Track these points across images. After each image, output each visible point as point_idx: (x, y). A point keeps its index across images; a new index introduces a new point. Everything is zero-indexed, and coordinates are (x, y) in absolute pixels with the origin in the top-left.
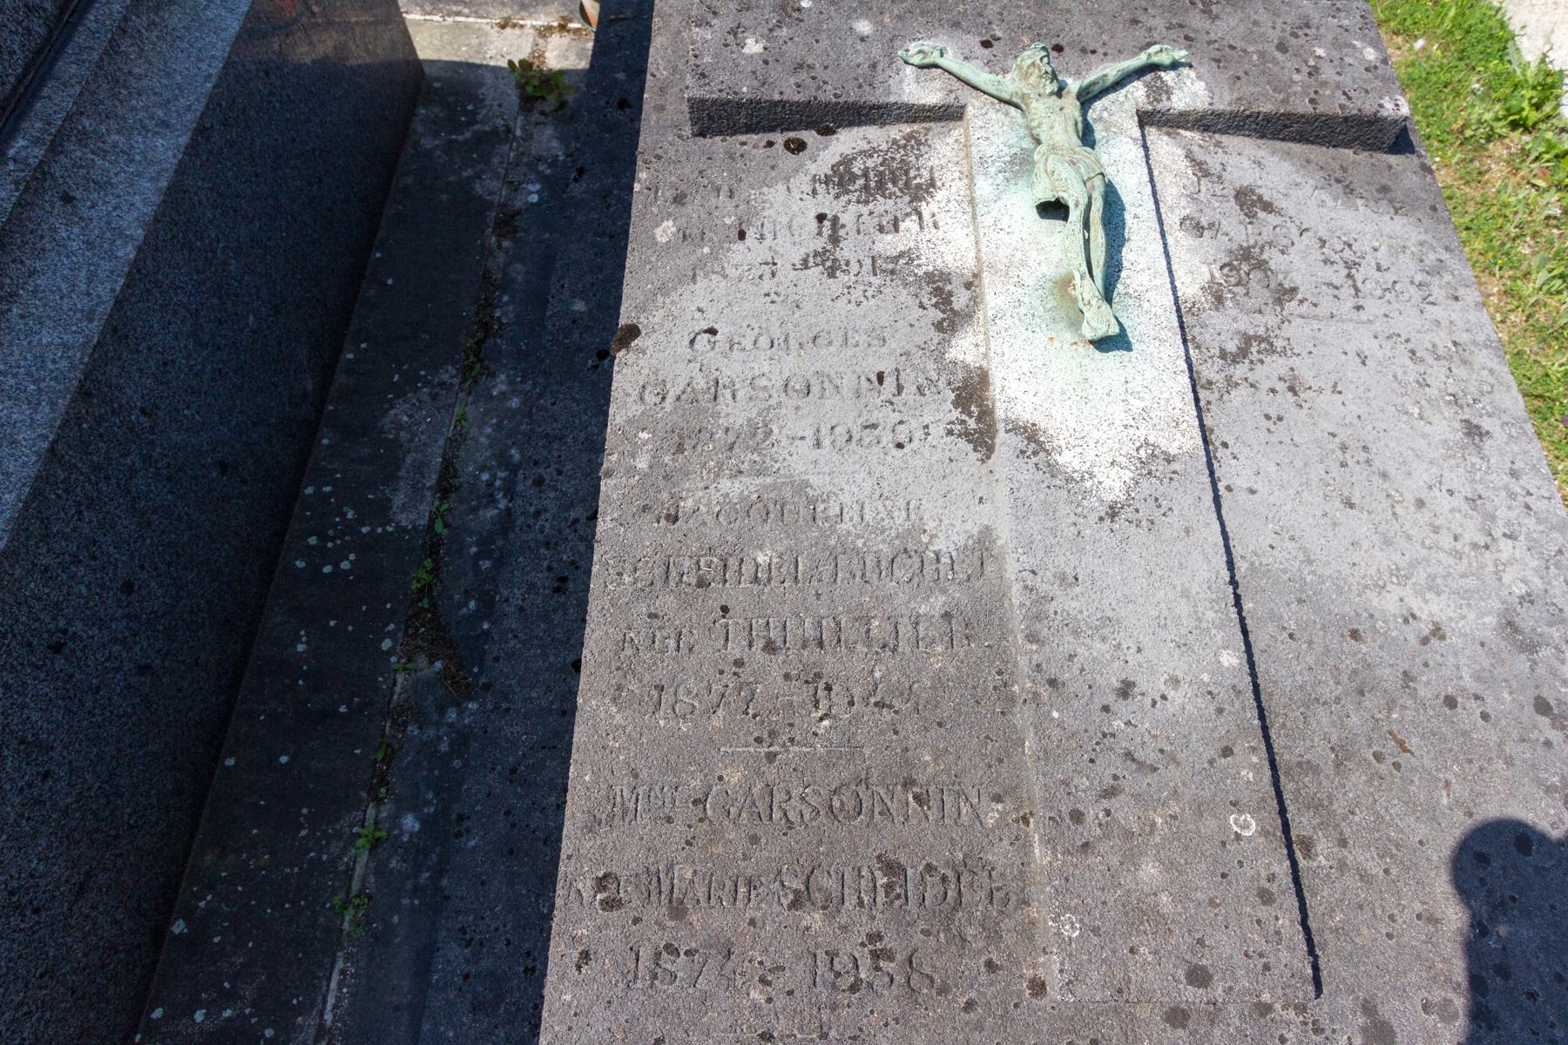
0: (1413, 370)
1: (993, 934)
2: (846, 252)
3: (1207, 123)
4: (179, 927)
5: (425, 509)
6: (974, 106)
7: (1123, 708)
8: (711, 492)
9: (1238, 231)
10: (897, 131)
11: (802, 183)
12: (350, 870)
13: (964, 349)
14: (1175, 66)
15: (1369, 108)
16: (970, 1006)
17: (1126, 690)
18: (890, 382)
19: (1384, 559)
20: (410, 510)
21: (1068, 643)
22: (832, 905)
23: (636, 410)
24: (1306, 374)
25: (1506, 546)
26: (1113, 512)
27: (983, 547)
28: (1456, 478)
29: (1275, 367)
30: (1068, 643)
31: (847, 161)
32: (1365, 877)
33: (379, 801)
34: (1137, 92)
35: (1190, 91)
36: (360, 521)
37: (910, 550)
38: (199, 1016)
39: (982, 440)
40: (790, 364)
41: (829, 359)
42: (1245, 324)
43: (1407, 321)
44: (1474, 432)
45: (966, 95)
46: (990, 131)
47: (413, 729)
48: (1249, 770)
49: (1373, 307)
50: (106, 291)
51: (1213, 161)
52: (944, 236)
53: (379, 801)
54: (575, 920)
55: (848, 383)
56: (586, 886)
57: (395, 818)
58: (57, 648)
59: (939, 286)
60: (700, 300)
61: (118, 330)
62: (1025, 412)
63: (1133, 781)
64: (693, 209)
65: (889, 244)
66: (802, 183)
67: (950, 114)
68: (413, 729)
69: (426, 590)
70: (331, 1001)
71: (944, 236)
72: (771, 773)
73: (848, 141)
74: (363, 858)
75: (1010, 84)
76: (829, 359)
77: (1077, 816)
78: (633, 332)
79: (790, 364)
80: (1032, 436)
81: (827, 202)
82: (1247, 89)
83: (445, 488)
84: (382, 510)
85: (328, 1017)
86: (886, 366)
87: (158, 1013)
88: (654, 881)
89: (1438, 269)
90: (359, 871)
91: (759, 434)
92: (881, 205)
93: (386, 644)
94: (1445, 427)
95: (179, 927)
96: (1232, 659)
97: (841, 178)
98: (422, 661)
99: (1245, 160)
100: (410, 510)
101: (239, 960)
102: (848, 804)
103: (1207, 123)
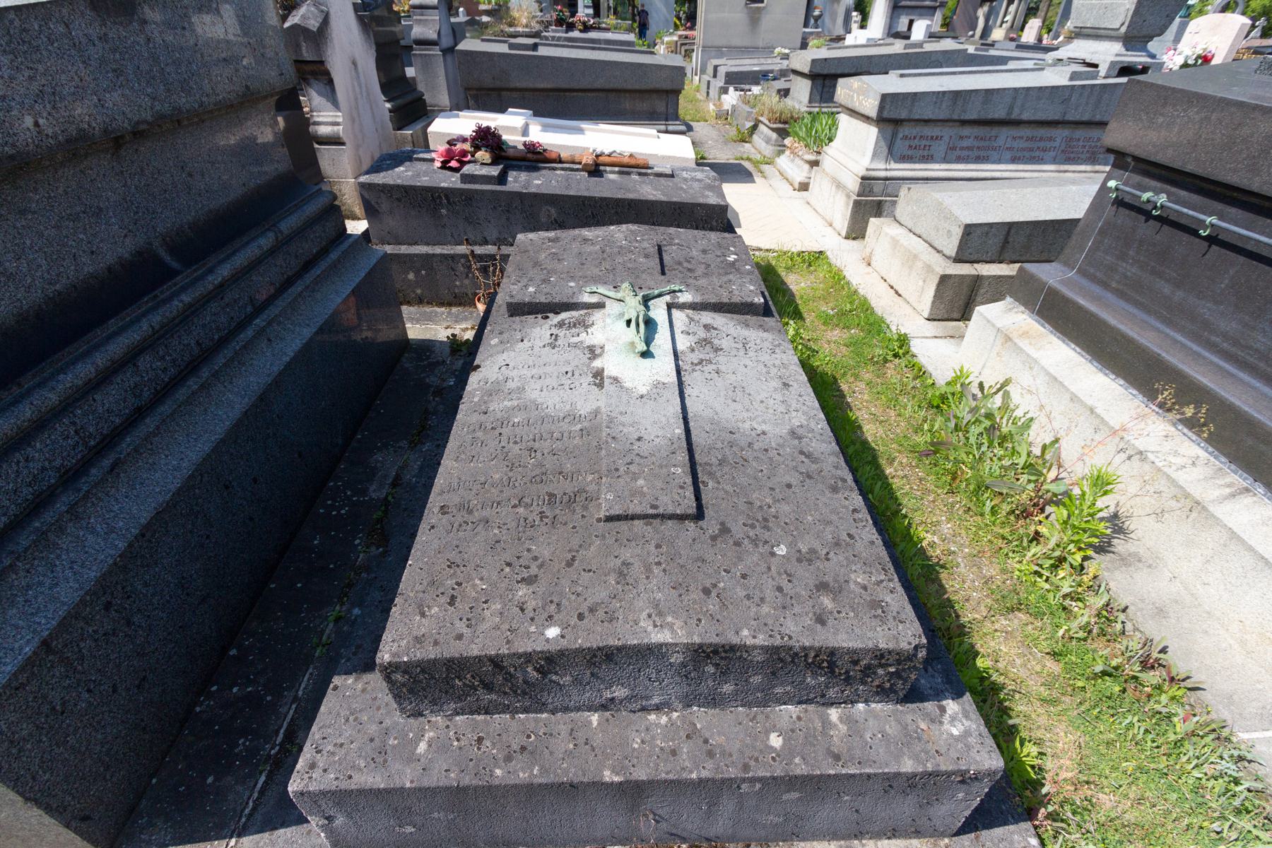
0: (765, 370)
1: (585, 508)
2: (559, 342)
3: (694, 306)
4: (233, 652)
5: (384, 492)
6: (608, 302)
7: (638, 444)
8: (498, 406)
9: (702, 334)
10: (582, 312)
11: (547, 326)
12: (323, 632)
13: (597, 364)
14: (680, 291)
15: (749, 300)
16: (574, 527)
17: (639, 439)
18: (570, 374)
19: (746, 415)
20: (376, 492)
21: (621, 428)
22: (527, 506)
23: (475, 386)
24: (723, 368)
25: (794, 414)
26: (642, 397)
27: (597, 412)
28: (779, 397)
29: (710, 367)
30: (621, 428)
31: (563, 320)
32: (726, 492)
33: (342, 604)
34: (667, 298)
35: (685, 297)
36: (352, 496)
37: (573, 417)
38: (235, 690)
39: (600, 386)
40: (534, 371)
41: (548, 369)
42: (702, 356)
43: (765, 357)
44: (786, 385)
45: (605, 299)
46: (612, 308)
47: (364, 575)
48: (683, 457)
49: (751, 354)
50: (276, 369)
51: (696, 318)
52: (595, 336)
53: (342, 604)
54: (432, 513)
55: (556, 374)
56: (436, 510)
57: (349, 611)
58: (227, 487)
59: (591, 349)
60: (501, 359)
61: (277, 382)
62: (614, 374)
63: (637, 460)
64: (505, 336)
65: (576, 339)
66: (547, 326)
67: (600, 306)
68: (364, 575)
69: (379, 521)
70: (303, 686)
71: (595, 336)
72: (511, 474)
73: (564, 315)
74: (331, 625)
75: (619, 296)
76: (548, 369)
77: (617, 470)
78: (478, 367)
79: (534, 371)
80: (616, 380)
81: (554, 331)
82: (706, 297)
83: (394, 484)
84: (364, 492)
85: (300, 693)
86: (569, 369)
87: (215, 688)
88: (461, 507)
89: (779, 345)
90: (327, 631)
91: (521, 389)
92: (574, 330)
93: (357, 542)
94: (776, 384)
95: (233, 652)
96: (679, 431)
97: (561, 325)
98: (373, 549)
99: (707, 317)
100: (376, 492)
101: (259, 667)
102: (540, 479)
103: (694, 306)
